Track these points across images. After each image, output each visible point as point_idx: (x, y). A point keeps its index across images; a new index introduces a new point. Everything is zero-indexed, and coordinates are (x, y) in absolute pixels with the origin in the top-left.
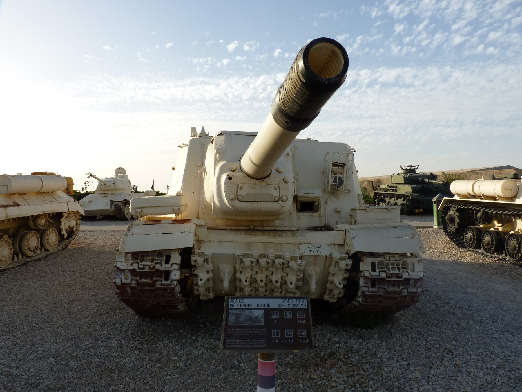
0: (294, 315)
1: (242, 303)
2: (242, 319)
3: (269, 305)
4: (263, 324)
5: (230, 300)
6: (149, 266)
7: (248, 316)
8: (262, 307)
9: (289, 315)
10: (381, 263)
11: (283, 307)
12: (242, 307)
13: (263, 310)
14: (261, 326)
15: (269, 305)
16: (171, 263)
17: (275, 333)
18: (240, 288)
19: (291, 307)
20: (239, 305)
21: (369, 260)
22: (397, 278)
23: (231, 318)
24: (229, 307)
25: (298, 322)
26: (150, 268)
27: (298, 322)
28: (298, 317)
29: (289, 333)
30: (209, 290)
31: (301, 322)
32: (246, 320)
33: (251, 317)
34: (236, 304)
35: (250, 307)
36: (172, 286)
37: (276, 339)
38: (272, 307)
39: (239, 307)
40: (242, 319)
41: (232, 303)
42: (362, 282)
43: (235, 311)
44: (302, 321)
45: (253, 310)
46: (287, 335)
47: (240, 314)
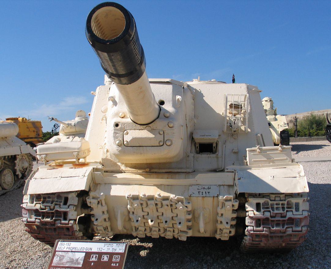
0: (110, 259)
1: (69, 246)
2: (64, 260)
3: (91, 249)
4: (81, 266)
5: (59, 243)
6: (50, 207)
7: (70, 258)
8: (85, 251)
9: (106, 258)
10: (266, 204)
11: (103, 251)
12: (67, 250)
15: (91, 249)
16: (68, 204)
18: (135, 227)
19: (109, 251)
20: (66, 248)
21: (254, 201)
22: (282, 217)
24: (57, 250)
26: (51, 209)
27: (112, 265)
28: (114, 260)
30: (107, 228)
31: (114, 265)
32: (67, 262)
33: (73, 259)
34: (63, 247)
35: (74, 250)
36: (70, 225)
38: (93, 251)
40: (64, 260)
42: (248, 221)
43: (60, 253)
44: (116, 264)
45: (75, 253)
47: (63, 256)
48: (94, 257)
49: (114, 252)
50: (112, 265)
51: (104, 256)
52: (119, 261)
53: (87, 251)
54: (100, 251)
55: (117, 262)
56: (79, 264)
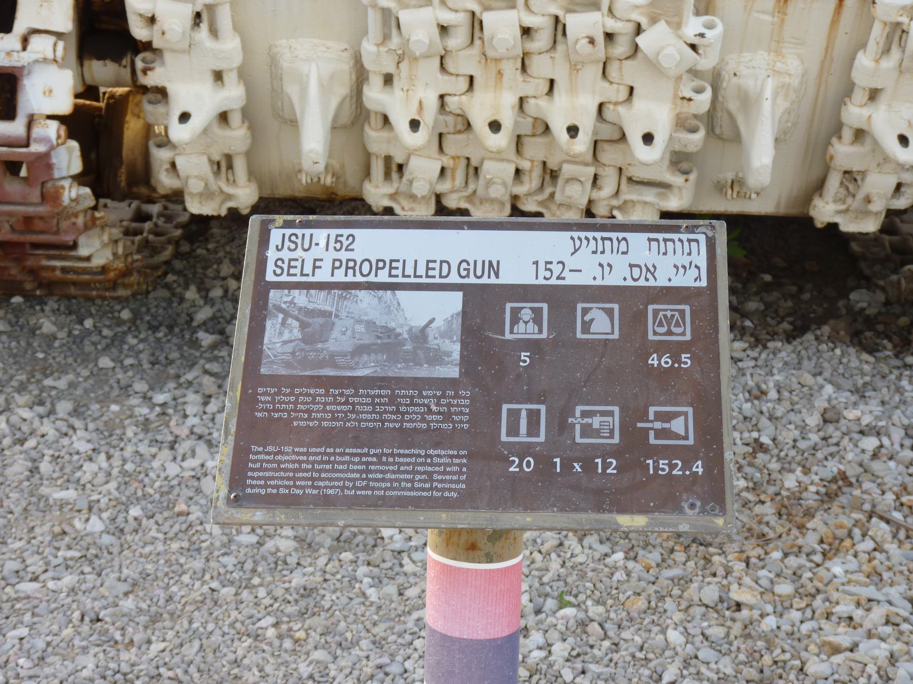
2: (339, 340)
3: (494, 268)
4: (453, 372)
7: (370, 324)
8: (454, 279)
9: (602, 324)
13: (459, 296)
14: (452, 383)
15: (494, 268)
17: (521, 425)
19: (614, 279)
23: (279, 338)
25: (653, 361)
27: (653, 361)
29: (596, 422)
31: (666, 361)
32: (360, 350)
33: (389, 331)
35: (383, 277)
37: (524, 451)
38: (508, 277)
39: (323, 276)
40: (339, 340)
41: (286, 255)
43: (300, 298)
45: (399, 293)
46: (587, 431)
47: (326, 314)
48: (526, 314)
49: (642, 283)
50: (656, 363)
51: (585, 311)
52: (688, 337)
53: (472, 280)
54: (553, 281)
55: (682, 347)
56: (437, 357)
